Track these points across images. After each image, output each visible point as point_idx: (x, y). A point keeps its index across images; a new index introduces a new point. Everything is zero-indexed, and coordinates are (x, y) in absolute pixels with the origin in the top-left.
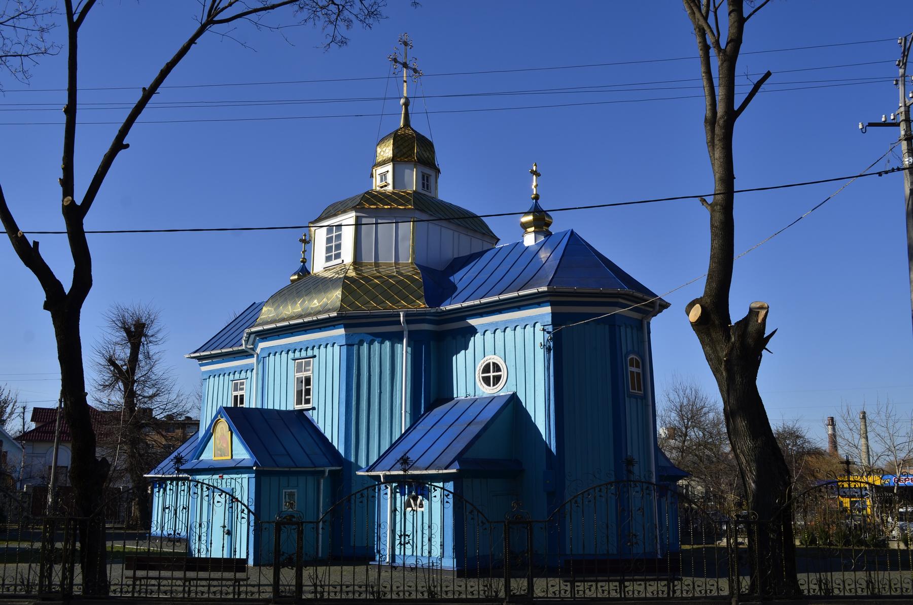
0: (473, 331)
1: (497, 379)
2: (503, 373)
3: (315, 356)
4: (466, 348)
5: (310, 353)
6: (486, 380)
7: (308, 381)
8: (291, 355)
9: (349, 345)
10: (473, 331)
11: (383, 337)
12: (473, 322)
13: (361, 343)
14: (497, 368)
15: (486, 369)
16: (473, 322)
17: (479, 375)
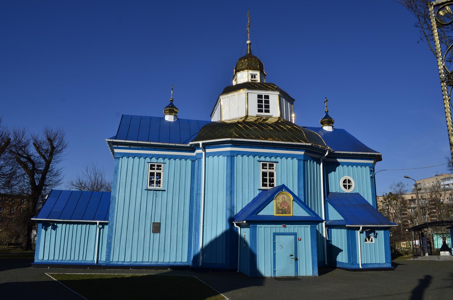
0: (338, 164)
1: (350, 187)
2: (353, 184)
3: (278, 162)
4: (335, 171)
5: (273, 159)
6: (345, 186)
7: (272, 175)
8: (257, 158)
9: (304, 161)
10: (338, 164)
11: (314, 159)
12: (339, 160)
13: (307, 161)
14: (349, 181)
15: (345, 181)
16: (339, 160)
17: (341, 184)
